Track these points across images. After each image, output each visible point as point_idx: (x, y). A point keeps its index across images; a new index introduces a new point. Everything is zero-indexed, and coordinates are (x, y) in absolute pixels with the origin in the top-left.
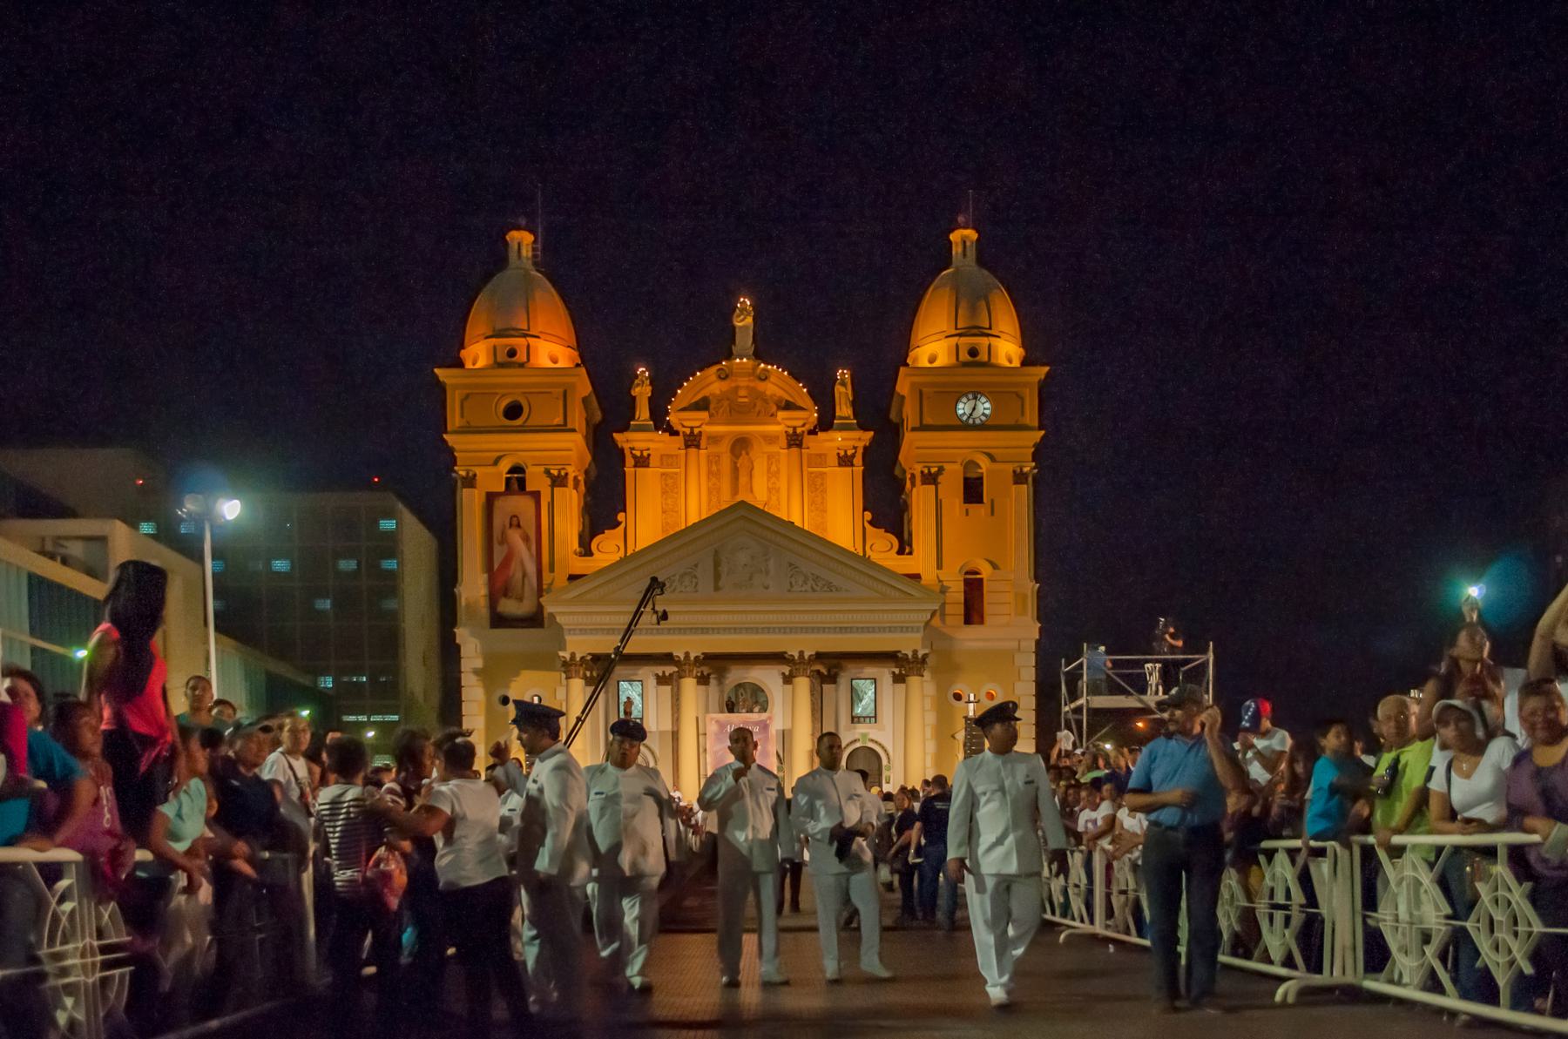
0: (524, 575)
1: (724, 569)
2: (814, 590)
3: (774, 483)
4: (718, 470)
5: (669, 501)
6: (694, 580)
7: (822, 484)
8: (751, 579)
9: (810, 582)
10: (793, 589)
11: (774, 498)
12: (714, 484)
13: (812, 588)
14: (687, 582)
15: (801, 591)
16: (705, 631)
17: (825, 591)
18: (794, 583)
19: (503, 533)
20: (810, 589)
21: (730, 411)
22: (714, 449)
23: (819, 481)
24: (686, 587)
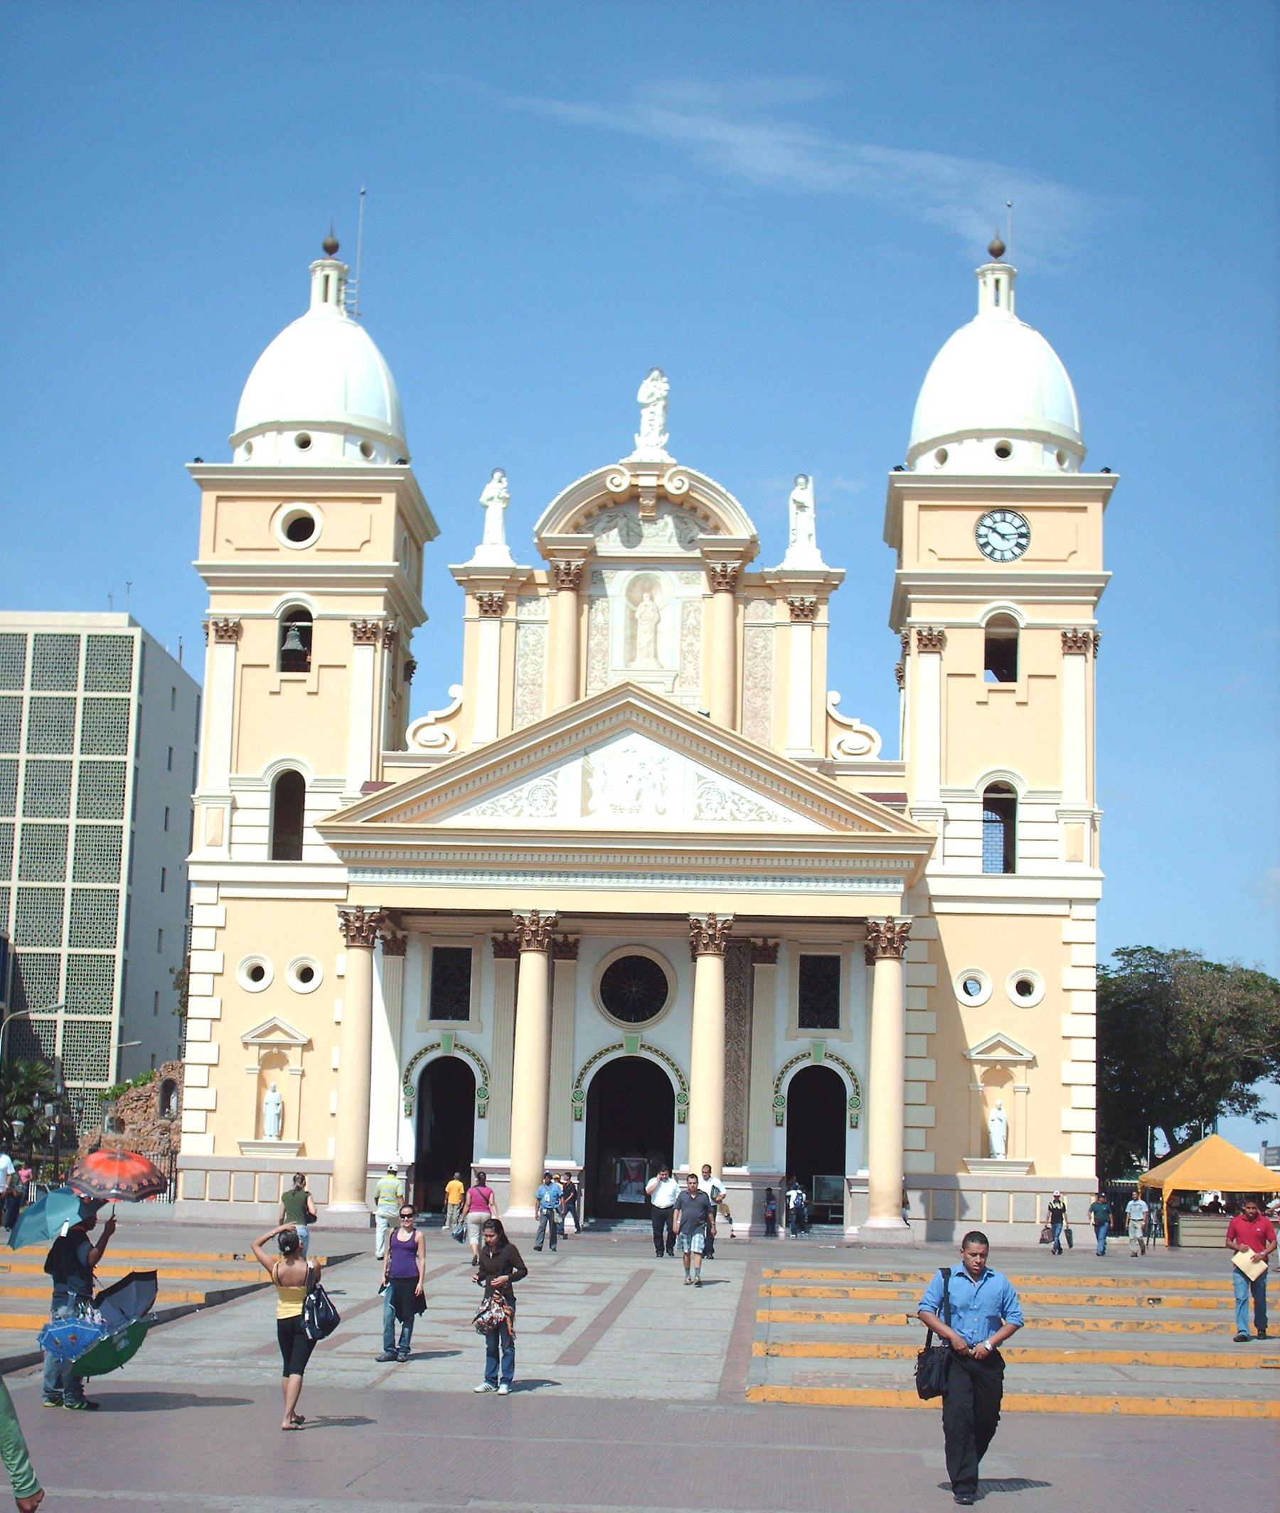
2: (735, 819)
3: (691, 644)
4: (606, 623)
5: (529, 669)
6: (551, 798)
7: (765, 647)
8: (639, 794)
9: (730, 806)
10: (703, 816)
11: (690, 668)
12: (600, 644)
13: (732, 814)
14: (539, 795)
15: (715, 819)
17: (754, 820)
18: (703, 807)
20: (726, 814)
21: (628, 535)
23: (761, 643)
24: (538, 809)
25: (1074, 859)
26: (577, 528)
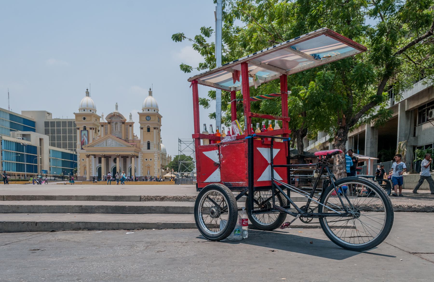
0: (86, 142)
1: (107, 143)
16: (105, 151)
19: (83, 136)
22: (112, 124)
25: (155, 148)
26: (110, 118)
